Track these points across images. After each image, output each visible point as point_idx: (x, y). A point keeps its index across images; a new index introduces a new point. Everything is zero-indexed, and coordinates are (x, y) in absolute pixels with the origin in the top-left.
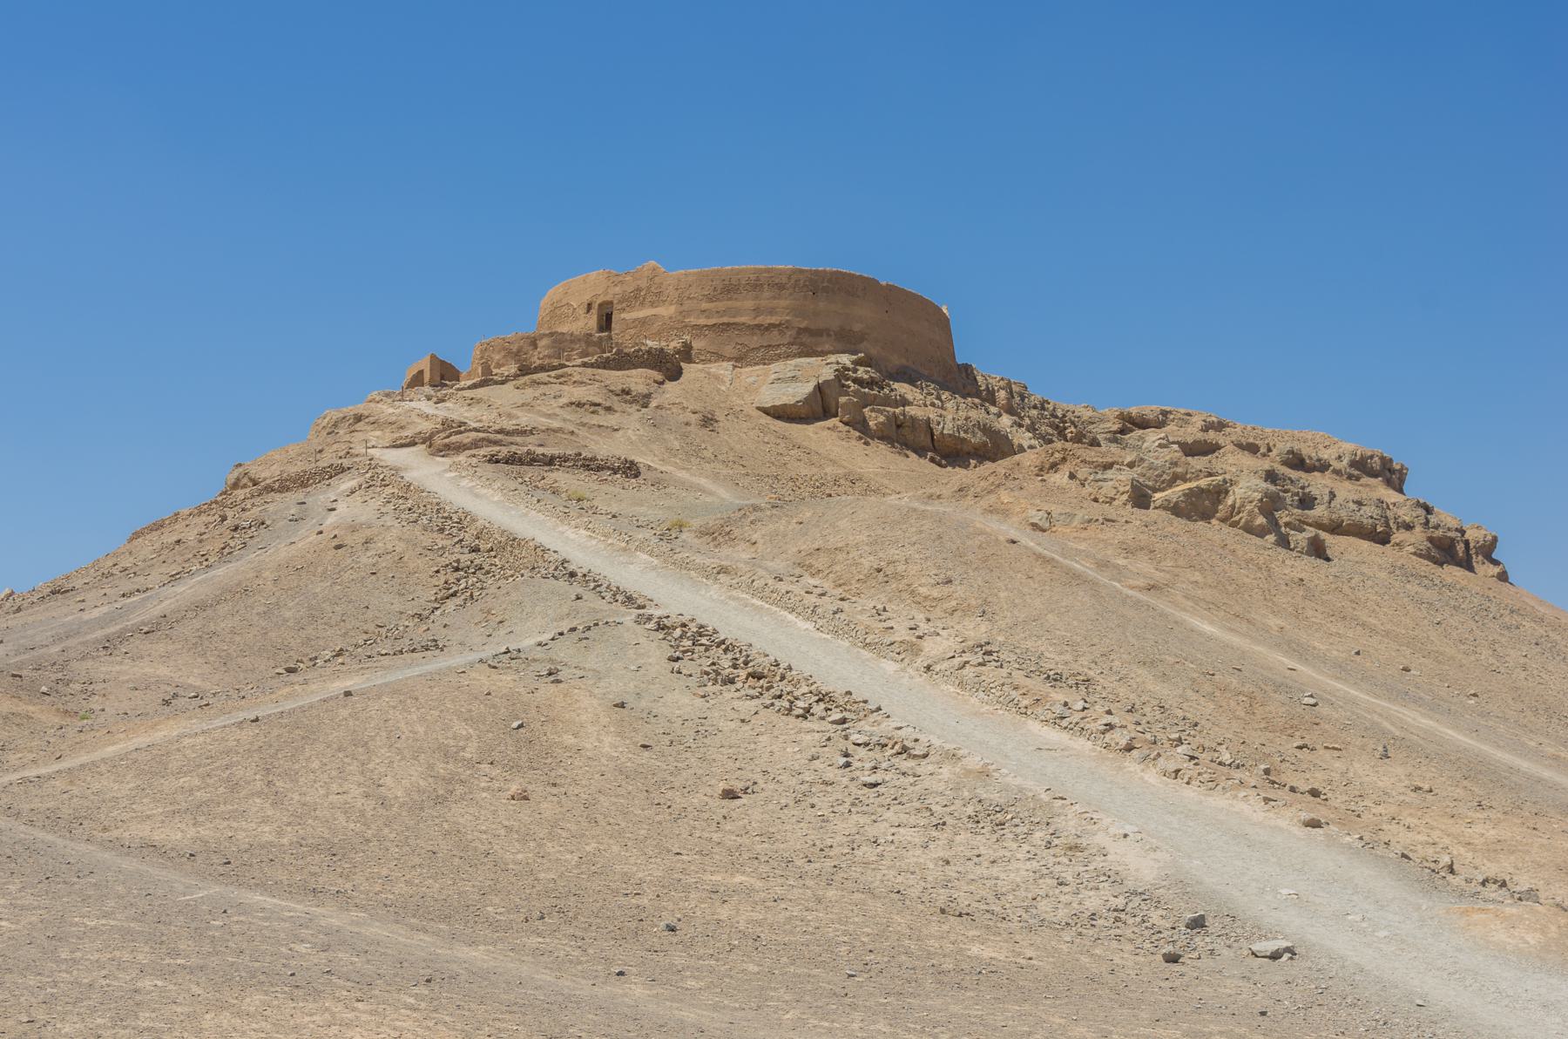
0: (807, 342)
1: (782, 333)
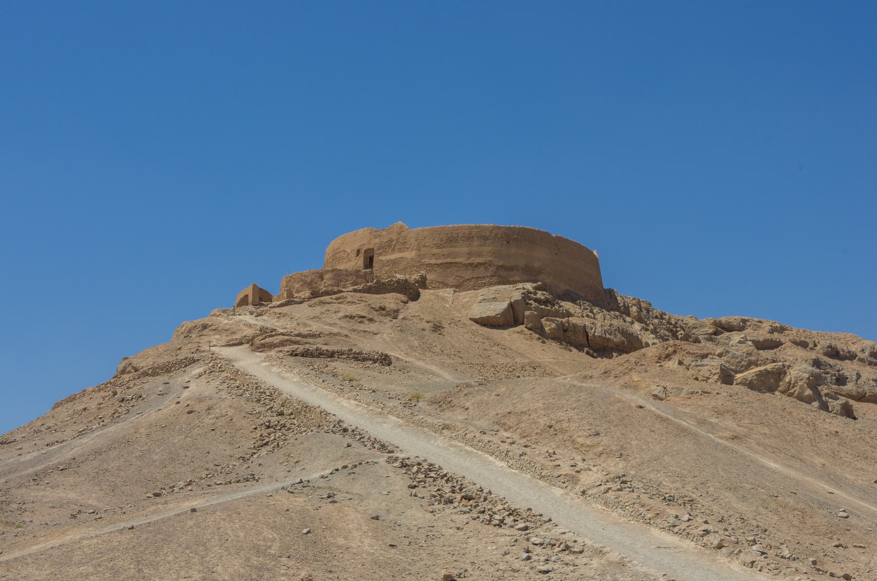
1: (486, 269)
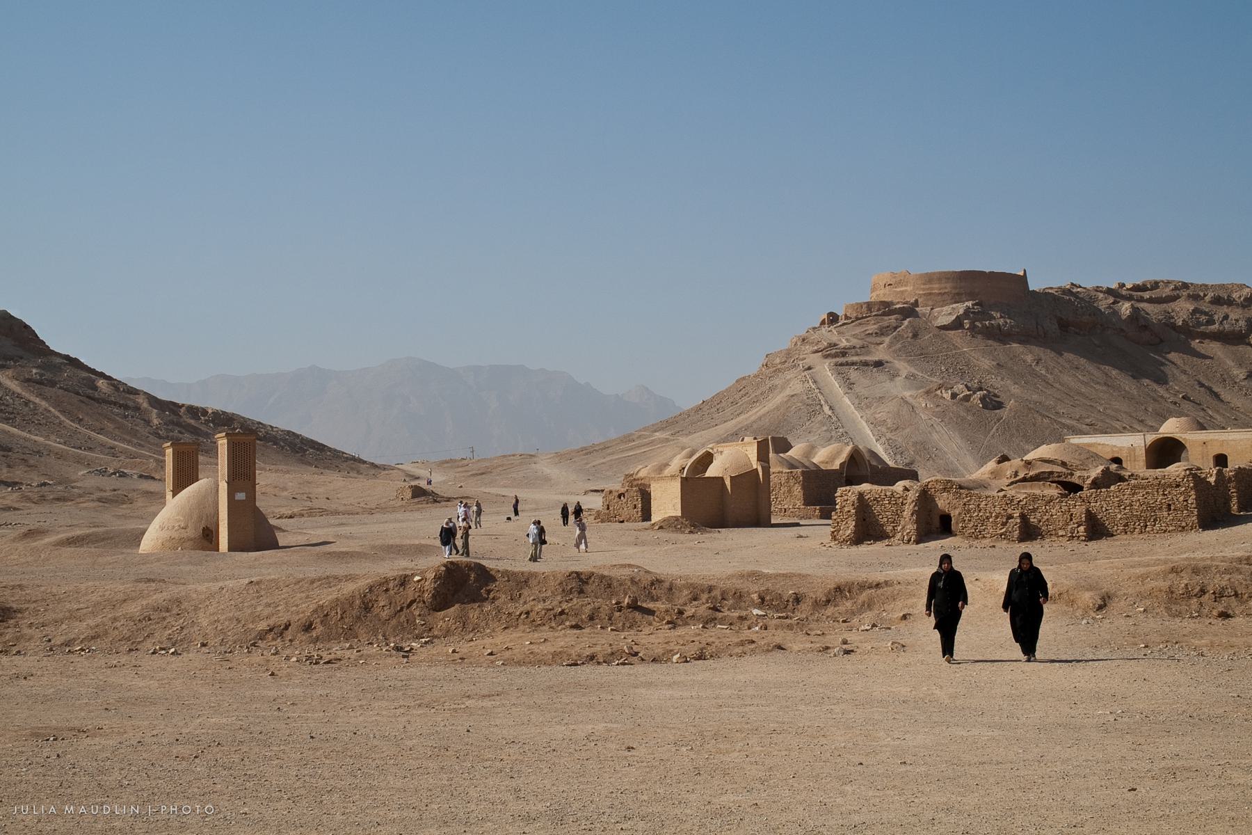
0: (957, 298)
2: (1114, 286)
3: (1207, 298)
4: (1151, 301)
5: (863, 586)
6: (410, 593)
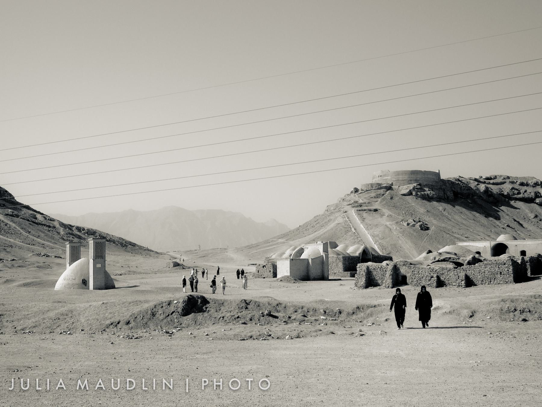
0: (410, 182)
2: (477, 177)
3: (518, 183)
4: (493, 184)
5: (369, 307)
6: (172, 309)
